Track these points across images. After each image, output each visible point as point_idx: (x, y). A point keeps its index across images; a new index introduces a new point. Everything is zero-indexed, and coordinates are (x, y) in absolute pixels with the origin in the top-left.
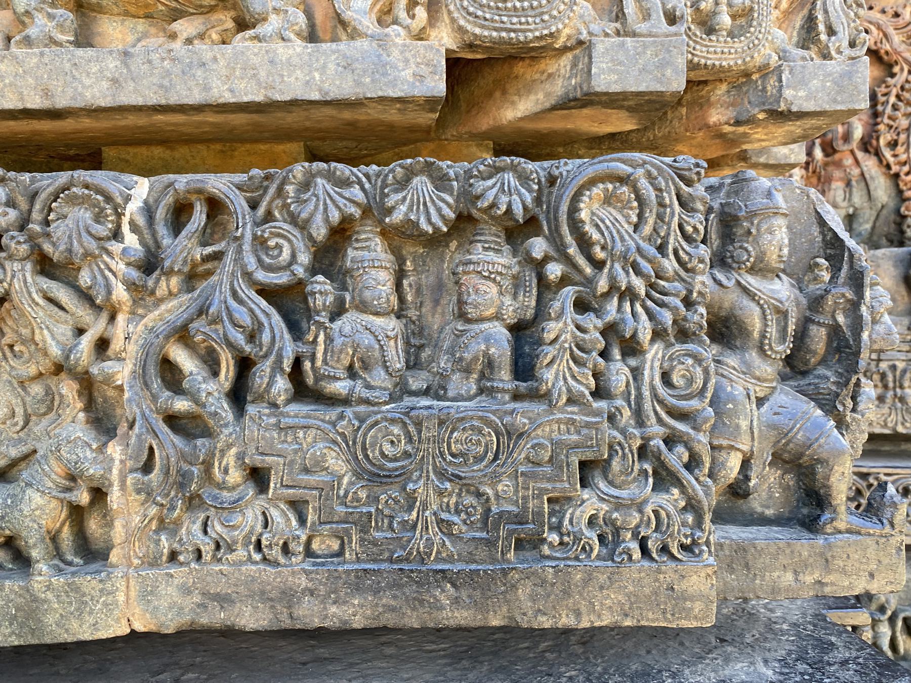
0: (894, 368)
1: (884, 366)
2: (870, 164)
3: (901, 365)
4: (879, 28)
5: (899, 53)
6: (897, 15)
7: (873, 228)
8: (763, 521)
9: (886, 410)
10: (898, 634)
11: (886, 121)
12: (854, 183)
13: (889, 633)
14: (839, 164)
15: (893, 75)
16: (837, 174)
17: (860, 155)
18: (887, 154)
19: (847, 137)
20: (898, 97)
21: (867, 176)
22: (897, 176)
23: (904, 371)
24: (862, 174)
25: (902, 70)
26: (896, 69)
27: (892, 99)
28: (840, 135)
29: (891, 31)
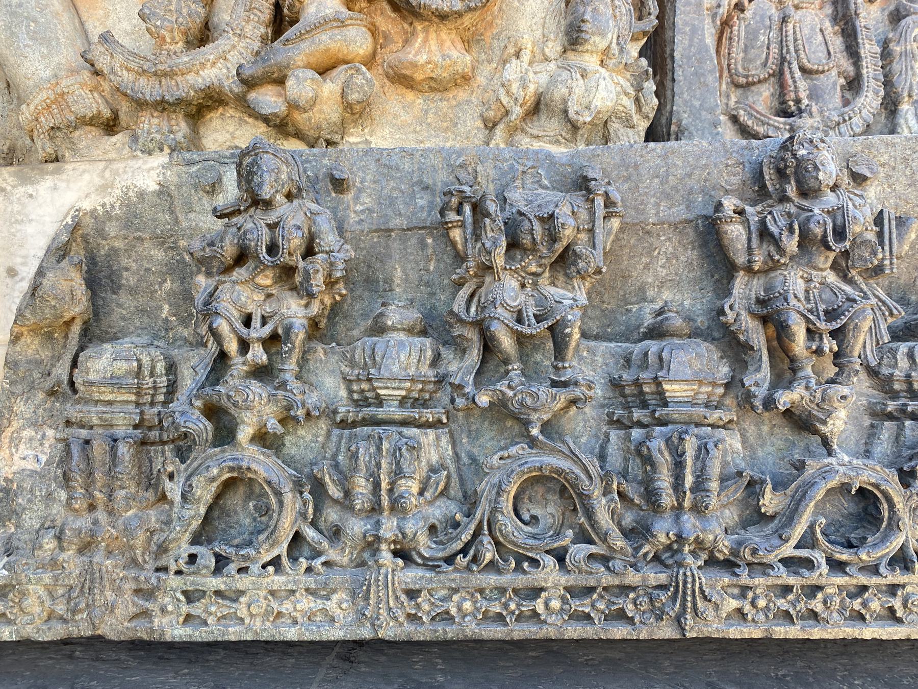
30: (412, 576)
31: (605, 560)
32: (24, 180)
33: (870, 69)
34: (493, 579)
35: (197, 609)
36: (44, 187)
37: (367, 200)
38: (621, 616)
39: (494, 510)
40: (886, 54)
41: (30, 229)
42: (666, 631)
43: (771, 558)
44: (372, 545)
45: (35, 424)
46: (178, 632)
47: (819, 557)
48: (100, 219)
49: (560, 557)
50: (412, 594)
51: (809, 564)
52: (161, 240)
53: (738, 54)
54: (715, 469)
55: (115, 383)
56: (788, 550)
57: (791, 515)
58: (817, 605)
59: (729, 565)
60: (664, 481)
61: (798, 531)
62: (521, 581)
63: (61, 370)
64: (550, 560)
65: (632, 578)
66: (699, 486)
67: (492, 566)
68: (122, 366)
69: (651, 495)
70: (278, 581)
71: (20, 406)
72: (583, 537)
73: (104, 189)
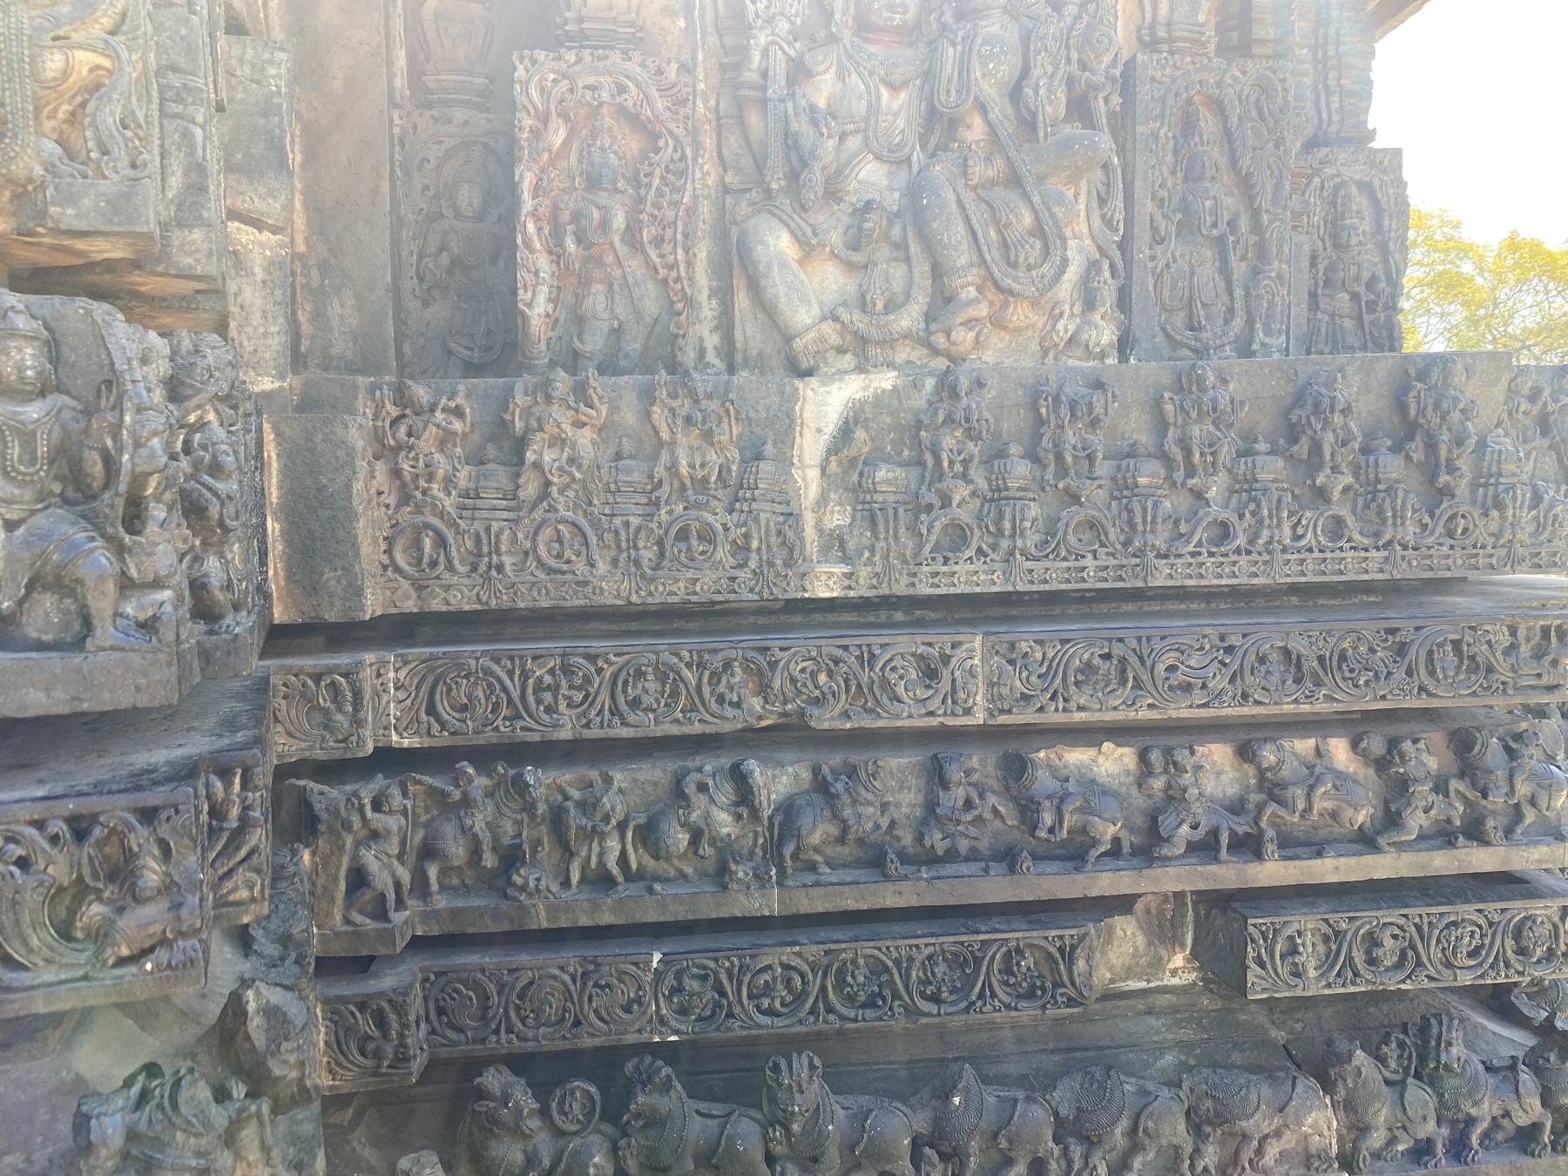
0: (627, 524)
1: (617, 521)
2: (634, 265)
3: (635, 521)
4: (638, 86)
5: (662, 122)
6: (659, 72)
7: (645, 348)
8: (41, 646)
9: (619, 576)
10: (630, 848)
11: (649, 208)
12: (616, 287)
13: (619, 847)
14: (599, 261)
15: (657, 151)
16: (597, 274)
17: (622, 250)
18: (653, 254)
19: (605, 225)
20: (662, 178)
21: (630, 280)
22: (665, 281)
23: (639, 529)
24: (624, 277)
25: (667, 144)
26: (661, 143)
27: (656, 182)
28: (595, 223)
29: (654, 92)
30: (1029, 564)
31: (1113, 555)
32: (823, 384)
33: (1239, 305)
34: (1065, 564)
35: (936, 580)
36: (834, 387)
37: (993, 392)
38: (1121, 579)
39: (1065, 533)
40: (1247, 295)
41: (829, 409)
42: (1140, 584)
43: (1184, 551)
44: (1011, 553)
45: (840, 504)
46: (929, 591)
47: (1204, 551)
48: (862, 403)
49: (1094, 553)
50: (1030, 571)
51: (1200, 554)
52: (891, 414)
53: (1166, 293)
54: (1160, 513)
55: (887, 482)
56: (1191, 548)
57: (1192, 533)
58: (1203, 571)
59: (1166, 556)
60: (1139, 519)
61: (1196, 539)
62: (1078, 564)
63: (855, 478)
64: (1090, 556)
65: (1124, 561)
66: (1153, 522)
67: (1065, 559)
68: (891, 475)
69: (1133, 526)
70: (972, 568)
71: (833, 496)
72: (1103, 545)
73: (865, 389)
